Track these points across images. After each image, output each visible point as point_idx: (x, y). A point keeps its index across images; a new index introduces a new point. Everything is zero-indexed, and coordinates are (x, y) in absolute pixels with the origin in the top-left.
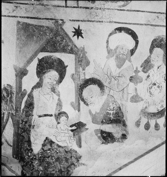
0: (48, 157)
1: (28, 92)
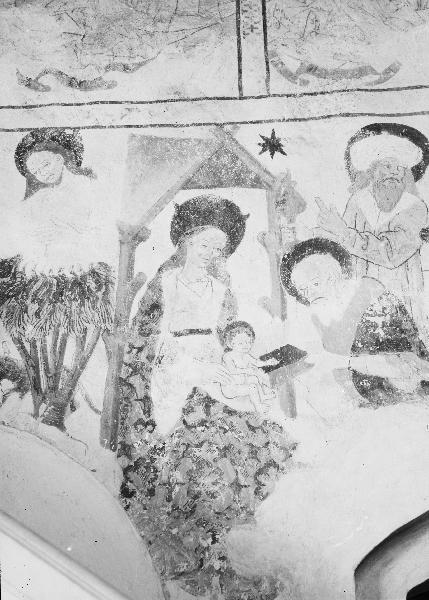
0: (200, 445)
1: (150, 276)
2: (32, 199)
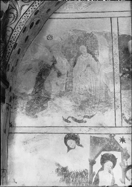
2: (69, 152)
